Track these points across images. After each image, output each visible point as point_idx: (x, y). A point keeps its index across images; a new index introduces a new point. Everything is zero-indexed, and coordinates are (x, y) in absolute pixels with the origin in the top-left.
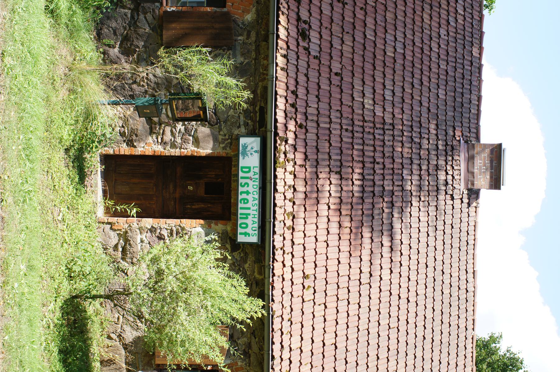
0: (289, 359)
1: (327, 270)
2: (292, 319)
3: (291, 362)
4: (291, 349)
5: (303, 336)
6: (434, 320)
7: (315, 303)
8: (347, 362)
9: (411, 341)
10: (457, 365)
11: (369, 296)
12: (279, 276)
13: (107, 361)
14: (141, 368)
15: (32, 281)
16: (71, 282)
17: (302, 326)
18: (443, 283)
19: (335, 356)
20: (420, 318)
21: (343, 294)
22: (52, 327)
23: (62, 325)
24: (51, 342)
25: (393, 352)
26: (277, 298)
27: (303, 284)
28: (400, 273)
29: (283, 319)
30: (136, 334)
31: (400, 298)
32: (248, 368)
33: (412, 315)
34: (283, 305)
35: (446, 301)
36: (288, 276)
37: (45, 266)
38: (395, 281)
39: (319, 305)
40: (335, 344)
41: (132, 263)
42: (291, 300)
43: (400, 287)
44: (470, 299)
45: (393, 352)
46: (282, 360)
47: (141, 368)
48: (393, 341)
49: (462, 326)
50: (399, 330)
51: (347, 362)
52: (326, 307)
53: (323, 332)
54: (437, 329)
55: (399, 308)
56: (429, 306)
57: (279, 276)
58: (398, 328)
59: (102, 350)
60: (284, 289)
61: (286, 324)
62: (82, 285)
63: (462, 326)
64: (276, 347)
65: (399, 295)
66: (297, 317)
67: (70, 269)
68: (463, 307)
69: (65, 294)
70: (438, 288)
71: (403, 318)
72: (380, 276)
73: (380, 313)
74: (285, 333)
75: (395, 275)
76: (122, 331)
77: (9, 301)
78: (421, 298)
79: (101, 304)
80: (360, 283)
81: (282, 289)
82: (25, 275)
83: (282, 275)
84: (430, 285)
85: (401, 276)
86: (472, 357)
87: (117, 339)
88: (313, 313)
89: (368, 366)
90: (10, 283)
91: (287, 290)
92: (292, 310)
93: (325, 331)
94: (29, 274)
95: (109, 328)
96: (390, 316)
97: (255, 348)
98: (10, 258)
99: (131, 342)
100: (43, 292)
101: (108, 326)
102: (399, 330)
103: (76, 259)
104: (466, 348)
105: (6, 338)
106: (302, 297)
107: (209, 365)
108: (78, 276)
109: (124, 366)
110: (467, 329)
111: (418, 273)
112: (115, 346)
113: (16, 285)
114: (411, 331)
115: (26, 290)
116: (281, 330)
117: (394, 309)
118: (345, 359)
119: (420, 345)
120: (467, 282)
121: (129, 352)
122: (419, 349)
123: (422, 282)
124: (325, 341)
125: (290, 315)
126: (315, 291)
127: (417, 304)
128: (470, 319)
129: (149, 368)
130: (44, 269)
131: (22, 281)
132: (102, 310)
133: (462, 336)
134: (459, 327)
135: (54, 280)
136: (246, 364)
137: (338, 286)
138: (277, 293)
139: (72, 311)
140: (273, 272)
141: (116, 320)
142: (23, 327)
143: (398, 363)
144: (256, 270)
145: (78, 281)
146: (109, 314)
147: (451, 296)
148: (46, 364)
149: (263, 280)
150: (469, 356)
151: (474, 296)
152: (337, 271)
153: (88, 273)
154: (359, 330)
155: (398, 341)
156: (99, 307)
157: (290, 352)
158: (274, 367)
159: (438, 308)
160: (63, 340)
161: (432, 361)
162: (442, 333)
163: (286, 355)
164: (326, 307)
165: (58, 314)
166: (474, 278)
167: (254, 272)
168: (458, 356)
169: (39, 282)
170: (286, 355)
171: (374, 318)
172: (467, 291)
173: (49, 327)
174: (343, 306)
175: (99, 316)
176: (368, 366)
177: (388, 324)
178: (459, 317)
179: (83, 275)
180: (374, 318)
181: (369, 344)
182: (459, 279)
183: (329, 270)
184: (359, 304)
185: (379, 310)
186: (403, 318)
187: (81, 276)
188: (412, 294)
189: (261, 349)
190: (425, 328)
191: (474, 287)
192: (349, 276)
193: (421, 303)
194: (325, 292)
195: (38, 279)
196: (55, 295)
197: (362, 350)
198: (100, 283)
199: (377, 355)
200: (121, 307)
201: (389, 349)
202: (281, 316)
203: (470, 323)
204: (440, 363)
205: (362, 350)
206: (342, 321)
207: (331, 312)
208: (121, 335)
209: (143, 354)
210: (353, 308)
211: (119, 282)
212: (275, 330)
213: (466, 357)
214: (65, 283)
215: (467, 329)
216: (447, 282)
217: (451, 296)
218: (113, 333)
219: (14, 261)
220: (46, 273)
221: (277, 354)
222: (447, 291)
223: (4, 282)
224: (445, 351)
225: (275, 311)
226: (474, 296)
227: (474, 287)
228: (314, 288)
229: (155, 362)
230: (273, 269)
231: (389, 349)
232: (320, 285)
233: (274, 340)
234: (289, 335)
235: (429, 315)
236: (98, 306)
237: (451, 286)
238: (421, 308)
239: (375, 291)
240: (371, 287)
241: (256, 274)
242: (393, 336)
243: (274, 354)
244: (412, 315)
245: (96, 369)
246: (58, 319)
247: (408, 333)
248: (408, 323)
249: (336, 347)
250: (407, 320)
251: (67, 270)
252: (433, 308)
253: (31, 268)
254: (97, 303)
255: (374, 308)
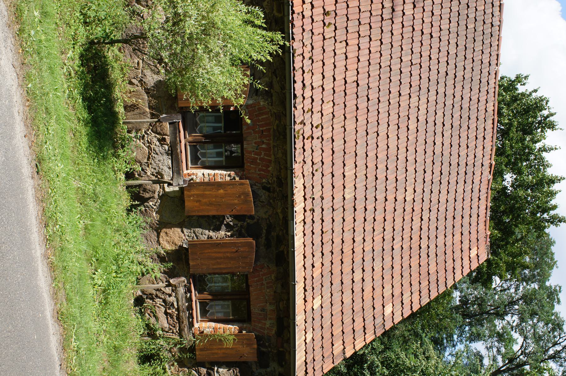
0: (311, 97)
1: (348, 5)
2: (313, 57)
3: (313, 100)
4: (312, 87)
5: (324, 74)
6: (457, 56)
7: (336, 41)
8: (368, 99)
9: (434, 77)
10: (479, 101)
11: (391, 31)
12: (298, 14)
13: (130, 107)
14: (164, 111)
15: (48, 28)
16: (88, 28)
17: (324, 64)
18: (468, 17)
19: (356, 93)
20: (444, 53)
21: (364, 30)
22: (73, 75)
23: (83, 72)
24: (74, 90)
25: (415, 88)
26: (298, 37)
27: (323, 21)
28: (423, 7)
29: (304, 57)
30: (157, 78)
31: (423, 33)
32: (271, 108)
33: (435, 51)
34: (303, 44)
35: (471, 36)
36: (307, 13)
37: (59, 12)
38: (418, 16)
39: (341, 42)
40: (357, 82)
41: (147, 6)
42: (312, 38)
43: (423, 22)
44: (495, 34)
45: (415, 88)
46: (304, 98)
47: (164, 111)
48: (416, 77)
49: (486, 61)
50: (421, 66)
51: (368, 99)
52: (347, 44)
53: (345, 70)
54: (460, 65)
55: (422, 44)
56: (453, 42)
57: (298, 14)
58: (420, 64)
59: (124, 95)
60: (304, 27)
61: (307, 62)
62: (98, 32)
63: (486, 61)
64: (298, 86)
65: (422, 30)
66: (318, 56)
67: (84, 15)
68: (487, 42)
69: (82, 40)
70: (462, 23)
71: (425, 54)
72: (403, 11)
73: (402, 49)
74: (306, 71)
75: (419, 10)
76: (143, 76)
77: (27, 49)
78: (445, 33)
79: (120, 50)
80: (382, 19)
81: (302, 26)
82: (40, 22)
83: (302, 12)
84: (454, 20)
85: (424, 10)
86: (494, 92)
87: (139, 84)
88: (334, 50)
89: (390, 103)
90: (27, 31)
91: (308, 27)
92: (313, 48)
93: (346, 69)
94: (44, 21)
95: (129, 73)
96: (412, 52)
97: (277, 87)
98: (23, 4)
99: (153, 87)
100: (60, 39)
101: (129, 72)
102: (421, 66)
103: (89, 4)
104: (488, 84)
105: (30, 86)
106: (323, 34)
107: (232, 106)
108: (94, 22)
109: (148, 110)
110: (490, 65)
111: (442, 7)
112: (137, 91)
113: (32, 33)
114: (434, 68)
115: (43, 38)
116: (302, 68)
117: (417, 45)
118: (367, 96)
119: (442, 81)
120: (493, 15)
121: (152, 97)
122: (442, 85)
123: (445, 17)
124: (346, 79)
125: (311, 53)
126: (336, 28)
127: (440, 40)
128: (494, 54)
129: (172, 111)
130: (58, 16)
131: (38, 29)
132: (121, 55)
133: (485, 71)
134: (482, 62)
135: (70, 27)
136: (268, 104)
137: (360, 22)
138: (297, 31)
139: (92, 58)
140: (292, 10)
141: (136, 65)
142: (45, 74)
143: (419, 99)
144: (275, 8)
145: (94, 27)
146: (128, 60)
147: (475, 30)
148: (71, 111)
149: (282, 18)
150: (491, 91)
151: (499, 31)
152: (359, 7)
153: (103, 18)
154: (380, 67)
155: (421, 78)
156: (118, 53)
157: (312, 90)
158: (296, 105)
159: (461, 43)
160: (86, 86)
161: (454, 97)
162: (465, 68)
163: (308, 94)
164: (347, 44)
165: (77, 62)
166: (500, 11)
167: (273, 10)
168: (480, 91)
169: (55, 29)
170: (308, 94)
171: (396, 55)
172: (492, 25)
173: (70, 75)
174: (364, 42)
175: (119, 62)
176: (390, 103)
177: (411, 61)
178: (483, 53)
179: (99, 20)
180: (396, 55)
181: (391, 80)
182: (485, 13)
183: (350, 6)
184: (381, 40)
185: (401, 46)
186: (425, 54)
187: (97, 21)
188: (436, 29)
189: (283, 88)
190: (448, 64)
191: (500, 21)
192: (370, 11)
193: (445, 38)
194: (346, 28)
195: (54, 26)
196: (73, 42)
197: (384, 87)
198: (116, 28)
199: (399, 92)
200: (141, 52)
201: (411, 86)
202: (302, 54)
203: (494, 58)
204: (462, 99)
205: (384, 87)
206: (364, 59)
207: (352, 48)
208: (142, 80)
209: (166, 98)
210: (375, 44)
211: (134, 27)
212: (296, 68)
213: (488, 93)
214: (82, 29)
215: (490, 65)
216: (472, 16)
217: (475, 30)
218: (134, 78)
219: (27, 8)
220: (61, 19)
221: (299, 92)
222: (471, 26)
223: (20, 30)
224: (467, 87)
225: (295, 50)
226: (499, 31)
227: (500, 21)
228: (335, 25)
229: (178, 105)
230: (292, 6)
231: (411, 86)
232: (341, 22)
233: (295, 79)
234: (311, 73)
235: (452, 51)
236: (117, 52)
237: (476, 20)
238: (444, 43)
239: (397, 26)
240: (393, 22)
241: (275, 12)
242: (415, 72)
243: (296, 92)
244: (435, 51)
245: (120, 115)
246: (79, 67)
247: (430, 69)
248: (430, 59)
249: (358, 85)
250: (429, 56)
251: (82, 17)
252: (456, 43)
253: (45, 14)
254: (115, 48)
255: (396, 45)
